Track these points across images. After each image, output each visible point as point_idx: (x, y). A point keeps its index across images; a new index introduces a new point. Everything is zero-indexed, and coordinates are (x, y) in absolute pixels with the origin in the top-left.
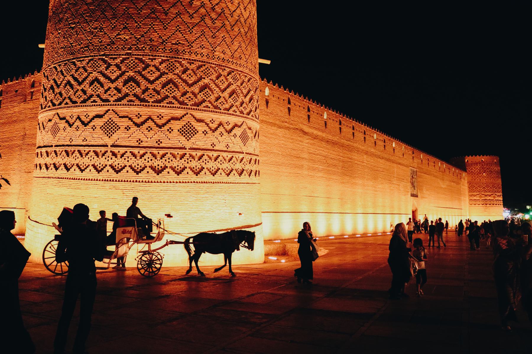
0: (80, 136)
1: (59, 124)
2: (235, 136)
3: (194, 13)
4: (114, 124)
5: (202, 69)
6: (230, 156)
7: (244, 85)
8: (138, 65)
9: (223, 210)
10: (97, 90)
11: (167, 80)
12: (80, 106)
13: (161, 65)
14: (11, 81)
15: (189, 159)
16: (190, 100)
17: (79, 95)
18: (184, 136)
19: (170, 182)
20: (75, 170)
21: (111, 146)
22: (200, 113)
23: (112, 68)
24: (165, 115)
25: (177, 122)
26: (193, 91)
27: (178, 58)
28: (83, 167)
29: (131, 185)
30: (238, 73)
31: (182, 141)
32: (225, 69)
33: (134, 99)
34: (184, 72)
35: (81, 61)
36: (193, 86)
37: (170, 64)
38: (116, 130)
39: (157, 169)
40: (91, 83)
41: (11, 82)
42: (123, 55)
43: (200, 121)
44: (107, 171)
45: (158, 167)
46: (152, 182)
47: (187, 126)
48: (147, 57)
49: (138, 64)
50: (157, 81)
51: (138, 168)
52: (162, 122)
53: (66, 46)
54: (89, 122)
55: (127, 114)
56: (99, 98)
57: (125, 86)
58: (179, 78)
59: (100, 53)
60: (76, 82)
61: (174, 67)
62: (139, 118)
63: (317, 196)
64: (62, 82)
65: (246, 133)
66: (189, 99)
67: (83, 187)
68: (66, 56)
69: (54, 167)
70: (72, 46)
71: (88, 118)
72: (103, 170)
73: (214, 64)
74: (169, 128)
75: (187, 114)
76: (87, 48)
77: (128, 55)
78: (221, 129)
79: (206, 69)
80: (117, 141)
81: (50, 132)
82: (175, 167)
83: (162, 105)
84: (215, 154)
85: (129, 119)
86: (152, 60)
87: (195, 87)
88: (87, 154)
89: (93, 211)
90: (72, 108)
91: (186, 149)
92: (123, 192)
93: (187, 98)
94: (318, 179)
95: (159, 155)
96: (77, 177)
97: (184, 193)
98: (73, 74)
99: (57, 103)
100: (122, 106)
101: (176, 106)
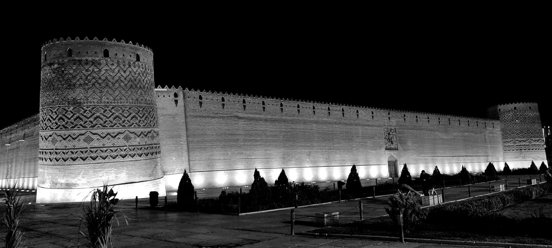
21: (55, 149)
25: (83, 136)
27: (81, 106)
30: (119, 107)
31: (85, 145)
32: (109, 107)
34: (85, 112)
46: (71, 165)
66: (88, 125)
73: (101, 106)
75: (87, 132)
78: (109, 136)
83: (74, 129)
86: (69, 108)
91: (88, 148)
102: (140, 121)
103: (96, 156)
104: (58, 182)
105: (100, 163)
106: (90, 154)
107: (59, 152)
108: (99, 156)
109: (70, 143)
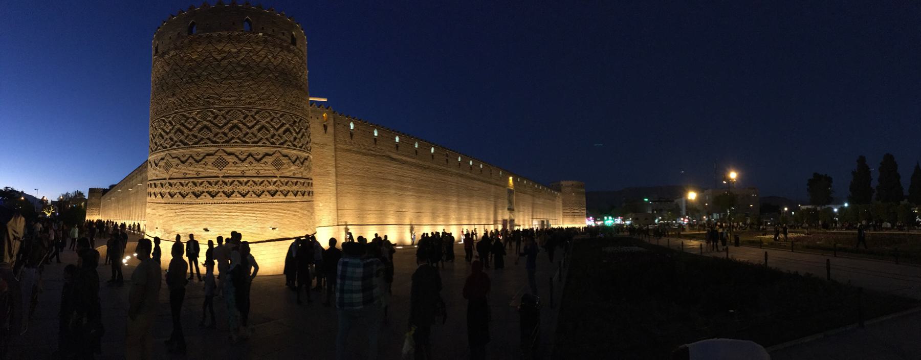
3: (222, 71)
5: (230, 113)
16: (221, 139)
18: (217, 167)
19: (207, 204)
25: (211, 157)
30: (266, 112)
31: (215, 171)
34: (215, 118)
43: (230, 154)
73: (240, 108)
75: (219, 150)
78: (250, 159)
84: (246, 180)
93: (219, 138)
102: (295, 139)
105: (237, 203)
106: (223, 186)
107: (174, 183)
109: (192, 168)
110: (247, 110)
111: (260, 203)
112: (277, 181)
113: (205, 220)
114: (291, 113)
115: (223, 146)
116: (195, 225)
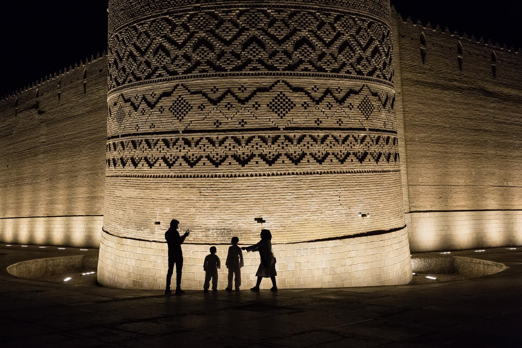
0: (146, 121)
1: (124, 108)
2: (351, 107)
4: (184, 104)
6: (344, 135)
7: (361, 33)
8: (209, 22)
9: (336, 211)
10: (162, 60)
11: (249, 38)
12: (144, 84)
13: (238, 19)
14: (95, 59)
15: (285, 143)
16: (281, 63)
17: (143, 69)
18: (276, 113)
19: (260, 175)
20: (143, 166)
21: (183, 132)
22: (296, 79)
23: (178, 29)
24: (249, 86)
25: (266, 94)
26: (286, 50)
28: (152, 161)
29: (209, 181)
30: (351, 18)
33: (207, 67)
34: (271, 25)
35: (142, 24)
36: (285, 43)
37: (250, 15)
38: (187, 110)
39: (242, 159)
40: (155, 53)
41: (94, 59)
42: (190, 10)
43: (296, 89)
44: (179, 165)
45: (244, 156)
46: (235, 176)
47: (279, 98)
48: (220, 9)
49: (210, 21)
50: (235, 41)
51: (217, 159)
52: (246, 96)
53: (125, 7)
54: (156, 103)
55: (200, 88)
56: (165, 71)
57: (195, 52)
58: (264, 34)
59: (163, 11)
60: (138, 53)
61: (256, 20)
62: (215, 92)
63: (512, 185)
64: (124, 54)
65: (368, 101)
66: (280, 61)
67: (153, 186)
68: (126, 20)
69: (121, 163)
70: (132, 6)
71: (154, 97)
72: (175, 163)
73: (313, 9)
74: (254, 103)
75: (279, 81)
76: (148, 7)
77: (196, 10)
78: (329, 99)
79: (302, 17)
80: (189, 125)
81: (115, 119)
82: (266, 155)
83: (243, 72)
84: (322, 134)
85: (203, 96)
86: (227, 12)
87: (288, 44)
88: (155, 144)
89: (165, 216)
90: (136, 86)
91: (279, 129)
92: (200, 191)
93: (277, 61)
94: (513, 161)
95: (244, 140)
96: (146, 174)
97: (279, 189)
98: (135, 43)
99: (120, 81)
100: (193, 79)
101: (263, 72)
103: (301, 153)
104: (195, 224)
105: (311, 173)
108: (308, 154)
109: (231, 113)
110: (324, 14)
111: (344, 173)
112: (366, 136)
113: (257, 203)
114: (379, 21)
115: (284, 74)
116: (241, 214)
